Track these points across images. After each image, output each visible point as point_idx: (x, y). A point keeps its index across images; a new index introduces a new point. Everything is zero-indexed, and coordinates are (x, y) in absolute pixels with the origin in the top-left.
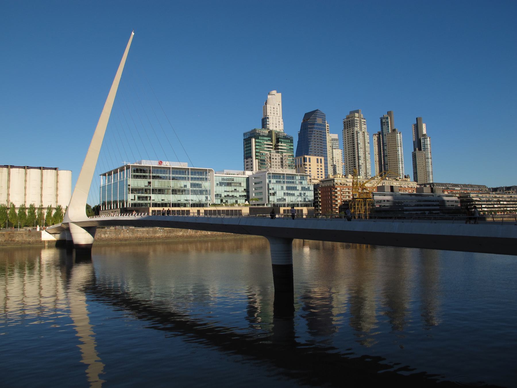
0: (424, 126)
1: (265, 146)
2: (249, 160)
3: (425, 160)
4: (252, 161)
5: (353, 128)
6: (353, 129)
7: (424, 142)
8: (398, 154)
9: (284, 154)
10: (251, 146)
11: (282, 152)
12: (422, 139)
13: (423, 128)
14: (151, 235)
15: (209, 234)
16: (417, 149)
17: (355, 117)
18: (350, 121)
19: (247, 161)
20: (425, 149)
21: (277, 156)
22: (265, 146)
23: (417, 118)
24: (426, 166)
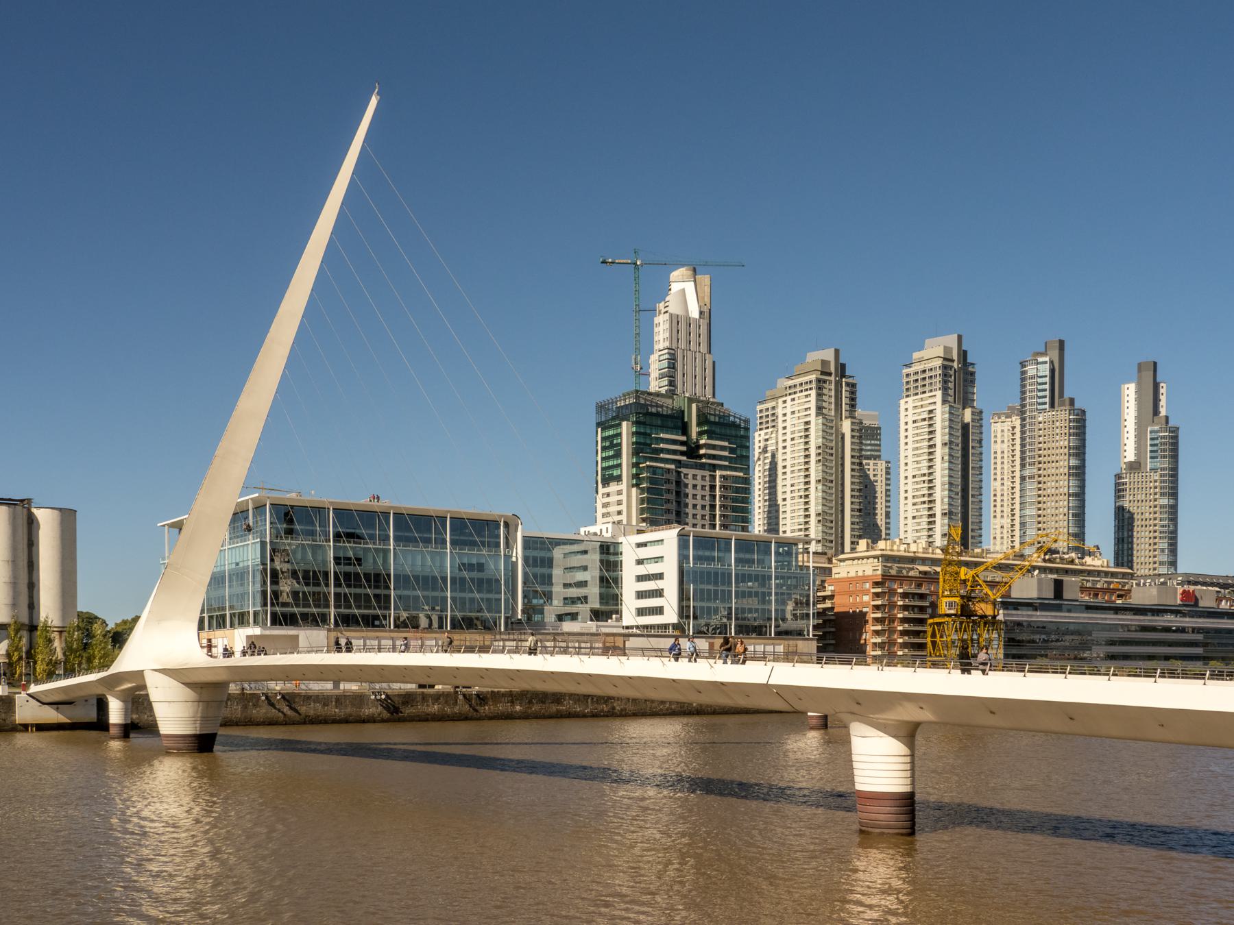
2: (613, 488)
14: (349, 710)
15: (516, 712)
19: (606, 490)
21: (699, 478)
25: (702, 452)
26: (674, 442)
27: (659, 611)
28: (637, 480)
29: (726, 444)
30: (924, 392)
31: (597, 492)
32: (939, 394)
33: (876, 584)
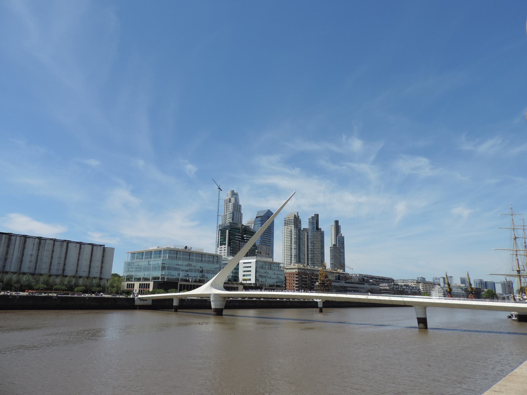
2: (223, 246)
19: (221, 247)
22: (236, 236)
25: (245, 238)
26: (239, 236)
27: (250, 280)
28: (229, 245)
30: (289, 225)
31: (218, 247)
32: (293, 226)
33: (296, 275)
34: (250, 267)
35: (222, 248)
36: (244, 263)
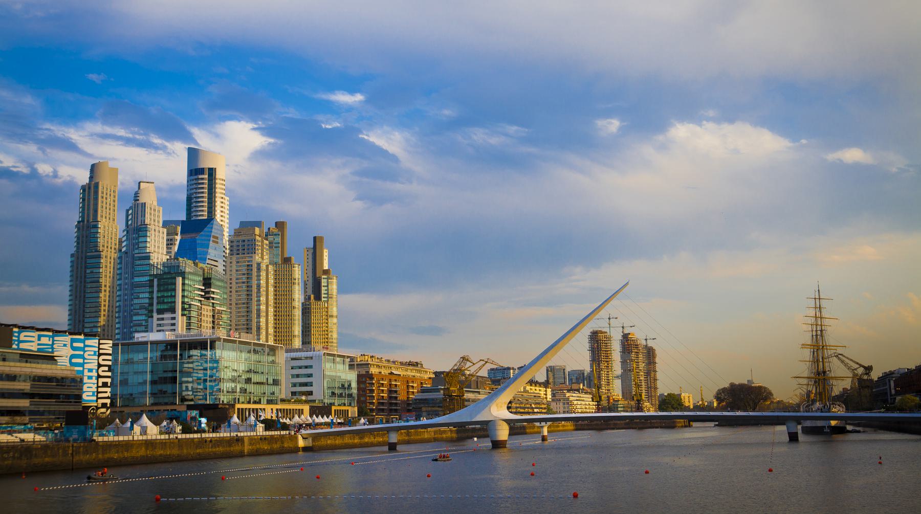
0: (326, 253)
1: (196, 292)
2: (167, 315)
3: (327, 320)
4: (174, 318)
5: (251, 255)
6: (251, 257)
7: (326, 284)
8: (294, 307)
9: (217, 307)
10: (175, 290)
11: (213, 303)
12: (323, 278)
13: (325, 257)
16: (312, 297)
17: (255, 235)
18: (244, 241)
20: (327, 297)
22: (196, 292)
23: (315, 238)
24: (327, 331)
29: (219, 291)
34: (311, 367)
35: (163, 319)
36: (293, 359)
